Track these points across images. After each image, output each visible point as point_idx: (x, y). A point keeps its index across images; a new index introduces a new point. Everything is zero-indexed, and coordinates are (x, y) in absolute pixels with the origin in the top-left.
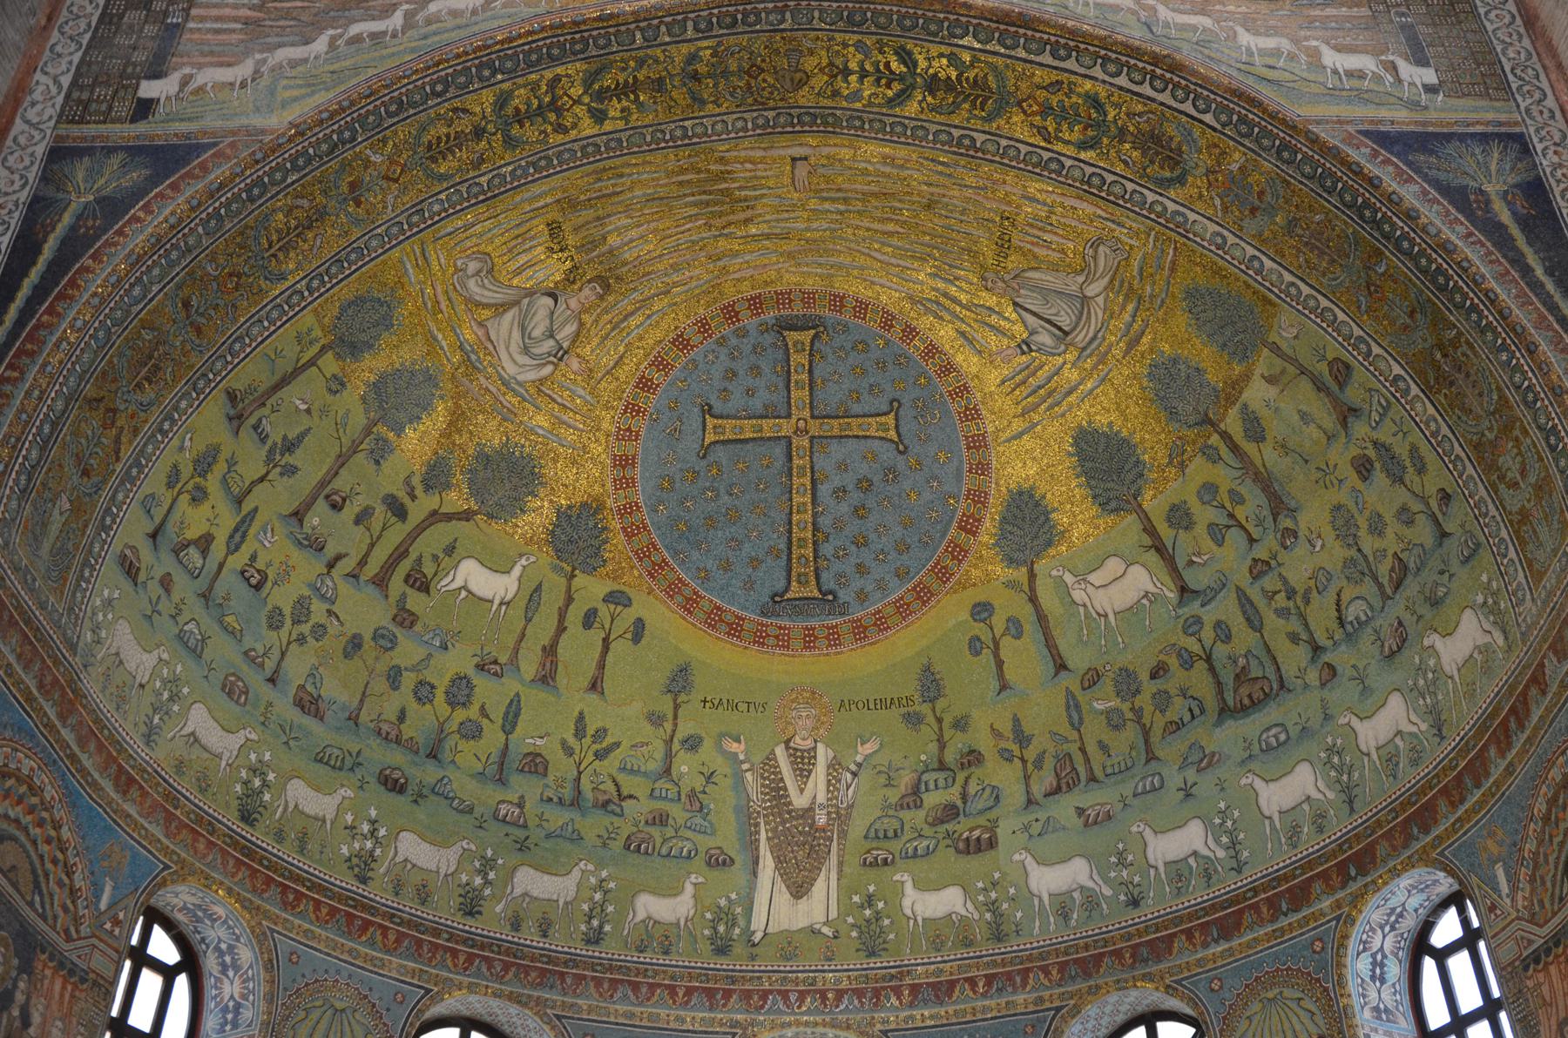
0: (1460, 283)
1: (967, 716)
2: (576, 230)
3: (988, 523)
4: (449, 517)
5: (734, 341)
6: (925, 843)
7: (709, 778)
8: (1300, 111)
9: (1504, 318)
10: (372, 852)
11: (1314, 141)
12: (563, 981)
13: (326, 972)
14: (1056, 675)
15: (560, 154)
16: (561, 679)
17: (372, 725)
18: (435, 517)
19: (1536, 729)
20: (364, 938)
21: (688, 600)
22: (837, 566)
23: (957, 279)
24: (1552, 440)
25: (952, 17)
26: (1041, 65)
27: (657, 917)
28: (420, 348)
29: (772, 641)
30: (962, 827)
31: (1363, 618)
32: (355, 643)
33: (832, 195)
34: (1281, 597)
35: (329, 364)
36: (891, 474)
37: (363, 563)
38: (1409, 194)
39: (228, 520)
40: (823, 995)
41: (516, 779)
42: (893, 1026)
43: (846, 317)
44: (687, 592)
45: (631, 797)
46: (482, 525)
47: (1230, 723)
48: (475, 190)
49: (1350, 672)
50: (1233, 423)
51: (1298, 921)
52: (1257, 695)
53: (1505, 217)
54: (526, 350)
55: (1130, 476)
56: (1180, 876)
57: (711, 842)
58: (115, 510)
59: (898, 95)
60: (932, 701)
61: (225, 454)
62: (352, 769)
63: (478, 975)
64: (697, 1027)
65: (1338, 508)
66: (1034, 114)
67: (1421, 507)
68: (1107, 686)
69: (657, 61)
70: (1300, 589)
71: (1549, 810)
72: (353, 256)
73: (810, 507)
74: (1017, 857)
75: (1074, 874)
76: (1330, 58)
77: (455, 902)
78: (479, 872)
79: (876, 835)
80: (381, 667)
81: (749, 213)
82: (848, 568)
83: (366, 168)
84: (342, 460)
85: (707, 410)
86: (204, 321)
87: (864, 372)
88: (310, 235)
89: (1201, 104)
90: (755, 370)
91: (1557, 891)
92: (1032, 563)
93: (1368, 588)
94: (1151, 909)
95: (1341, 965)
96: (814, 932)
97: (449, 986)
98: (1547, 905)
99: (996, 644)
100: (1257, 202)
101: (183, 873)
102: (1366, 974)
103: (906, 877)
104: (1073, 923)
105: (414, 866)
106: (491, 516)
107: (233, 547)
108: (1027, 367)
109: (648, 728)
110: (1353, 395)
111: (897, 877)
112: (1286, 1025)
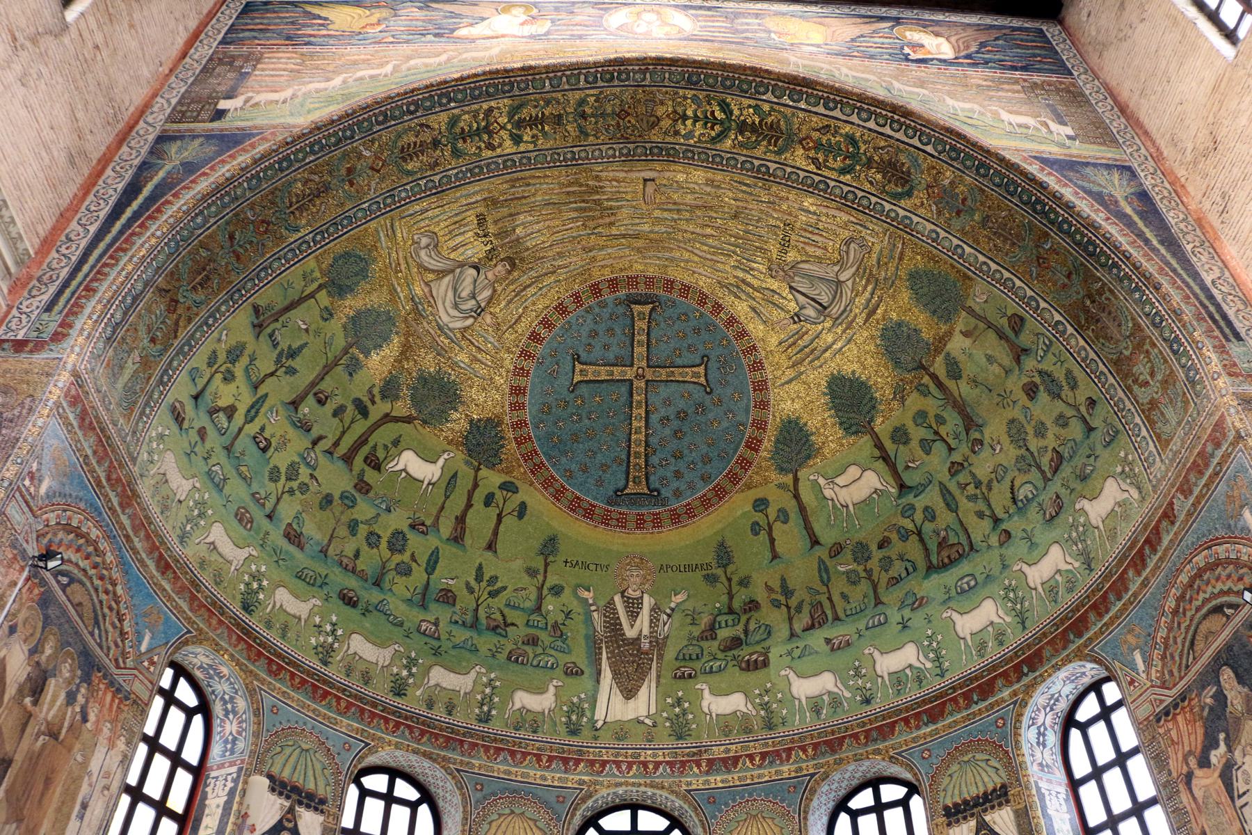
2: (496, 222)
4: (397, 420)
5: (597, 310)
6: (718, 663)
7: (568, 615)
9: (1137, 269)
10: (331, 645)
11: (1002, 160)
12: (462, 746)
15: (488, 165)
16: (468, 541)
18: (387, 418)
19: (1167, 550)
21: (557, 491)
22: (661, 472)
23: (752, 269)
24: (1175, 347)
26: (816, 113)
27: (529, 707)
30: (744, 653)
31: (1030, 496)
32: (327, 500)
33: (670, 206)
34: (971, 489)
36: (700, 407)
38: (1068, 193)
39: (246, 400)
40: (645, 764)
41: (433, 606)
42: (694, 787)
43: (675, 295)
44: (557, 486)
45: (513, 624)
47: (935, 576)
48: (430, 185)
49: (1021, 534)
51: (986, 707)
55: (866, 409)
57: (568, 658)
59: (718, 135)
60: (725, 566)
61: (247, 352)
63: (402, 736)
64: (556, 784)
65: (1012, 421)
66: (809, 149)
67: (1075, 413)
68: (848, 555)
69: (558, 102)
70: (985, 482)
71: (1178, 606)
73: (643, 430)
74: (783, 673)
75: (826, 682)
78: (406, 667)
79: (682, 658)
80: (344, 519)
81: (612, 219)
83: (359, 159)
84: (327, 369)
85: (577, 358)
87: (685, 336)
93: (1034, 475)
94: (877, 706)
95: (1017, 734)
100: (961, 207)
101: (200, 639)
102: (1034, 741)
103: (704, 686)
104: (823, 716)
106: (425, 422)
107: (249, 419)
109: (527, 578)
110: (1025, 339)
111: (698, 686)
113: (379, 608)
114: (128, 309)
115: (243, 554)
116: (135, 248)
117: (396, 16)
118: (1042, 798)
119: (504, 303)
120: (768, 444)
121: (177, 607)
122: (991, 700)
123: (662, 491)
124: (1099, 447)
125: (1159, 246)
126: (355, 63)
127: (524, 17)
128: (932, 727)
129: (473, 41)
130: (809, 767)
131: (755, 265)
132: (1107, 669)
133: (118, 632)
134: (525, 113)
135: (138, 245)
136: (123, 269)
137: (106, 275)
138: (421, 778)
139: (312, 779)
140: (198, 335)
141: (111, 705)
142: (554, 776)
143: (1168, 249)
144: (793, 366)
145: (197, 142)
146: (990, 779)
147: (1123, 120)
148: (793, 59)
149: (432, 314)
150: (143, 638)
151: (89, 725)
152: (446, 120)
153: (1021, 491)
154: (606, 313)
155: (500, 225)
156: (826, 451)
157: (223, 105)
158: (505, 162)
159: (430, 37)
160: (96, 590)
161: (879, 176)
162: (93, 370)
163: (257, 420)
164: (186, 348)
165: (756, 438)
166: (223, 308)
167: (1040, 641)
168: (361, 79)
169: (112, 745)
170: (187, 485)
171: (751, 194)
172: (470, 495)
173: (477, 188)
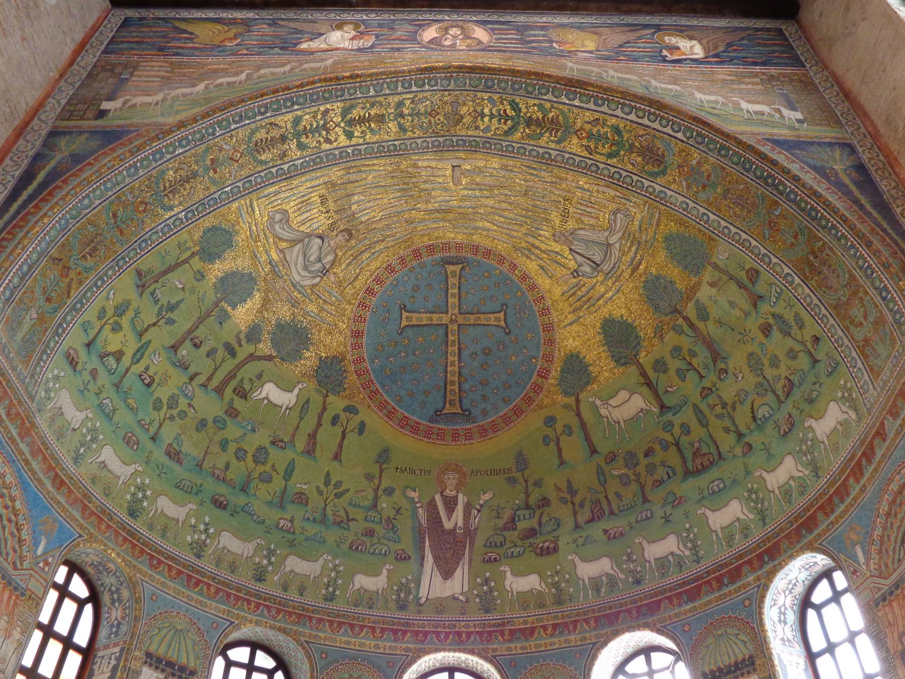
0: (825, 213)
3: (553, 373)
4: (260, 358)
5: (418, 270)
6: (518, 550)
7: (398, 511)
11: (739, 142)
13: (173, 607)
14: (591, 455)
15: (328, 155)
16: (318, 452)
17: (210, 470)
18: (252, 357)
19: (880, 462)
20: (196, 590)
21: (390, 412)
23: (540, 236)
24: (884, 294)
25: (541, 83)
26: (588, 109)
27: (366, 587)
28: (247, 263)
29: (435, 436)
30: (539, 541)
31: (767, 415)
32: (203, 424)
35: (196, 263)
37: (210, 379)
38: (795, 168)
40: (459, 634)
42: (499, 653)
43: (479, 257)
44: (389, 408)
45: (354, 520)
46: (278, 364)
48: (280, 172)
52: (706, 463)
53: (847, 181)
54: (306, 268)
56: (663, 566)
57: (398, 547)
58: (65, 326)
59: (510, 129)
60: (523, 470)
61: (134, 306)
62: (196, 494)
64: (387, 651)
65: (751, 354)
66: (582, 139)
68: (620, 461)
69: (381, 104)
70: (730, 403)
71: (890, 509)
72: (212, 202)
74: (570, 557)
75: (603, 566)
76: (744, 105)
77: (251, 573)
78: (266, 557)
79: (490, 545)
80: (217, 439)
83: (220, 151)
84: (201, 320)
85: (404, 308)
86: (124, 226)
90: (430, 285)
91: (897, 557)
92: (578, 394)
93: (770, 398)
94: (648, 586)
95: (761, 614)
96: (454, 598)
98: (891, 566)
99: (558, 439)
100: (706, 182)
102: (776, 619)
104: (602, 594)
105: (228, 551)
107: (136, 360)
108: (577, 285)
110: (760, 288)
111: (502, 569)
112: (730, 650)
114: (24, 275)
115: (131, 469)
116: (30, 225)
117: (249, 31)
118: (784, 668)
119: (343, 267)
120: (555, 373)
123: (473, 411)
125: (871, 210)
126: (215, 71)
127: (353, 33)
128: (690, 606)
129: (312, 53)
131: (542, 232)
132: (834, 560)
134: (355, 113)
135: (32, 223)
136: (19, 243)
138: (277, 649)
139: (185, 655)
140: (89, 294)
141: (8, 601)
142: (386, 644)
143: (880, 213)
145: (83, 137)
146: (740, 650)
147: (846, 104)
148: (570, 64)
150: (39, 544)
152: (291, 120)
153: (760, 411)
155: (339, 202)
157: (105, 105)
158: (340, 153)
163: (142, 361)
164: (78, 306)
165: (545, 369)
168: (221, 85)
170: (80, 416)
171: (537, 176)
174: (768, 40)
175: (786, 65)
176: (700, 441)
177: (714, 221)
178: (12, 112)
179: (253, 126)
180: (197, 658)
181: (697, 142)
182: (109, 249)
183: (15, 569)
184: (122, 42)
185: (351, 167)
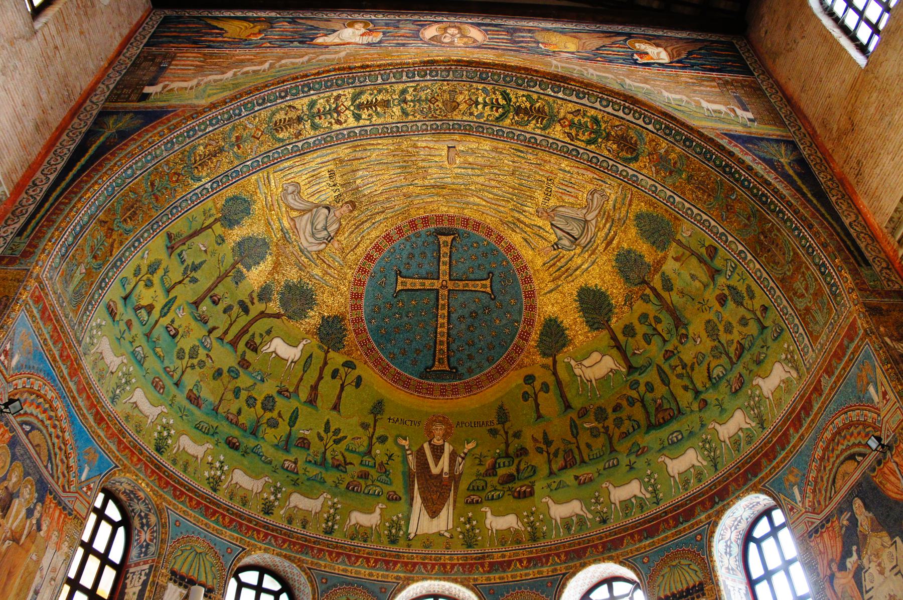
1: (521, 431)
5: (414, 239)
7: (390, 457)
8: (694, 123)
10: (220, 477)
11: (701, 135)
15: (337, 135)
18: (262, 315)
19: (816, 414)
21: (384, 368)
22: (458, 355)
23: (525, 211)
24: (823, 270)
27: (361, 523)
30: (517, 486)
32: (219, 373)
35: (218, 228)
37: (226, 333)
39: (161, 301)
40: (444, 565)
41: (293, 450)
42: (479, 582)
43: (469, 229)
45: (351, 464)
46: (285, 322)
48: (295, 149)
50: (657, 282)
53: (791, 172)
54: (313, 235)
55: (605, 312)
59: (501, 116)
61: (162, 266)
62: (213, 435)
63: (270, 543)
64: (380, 579)
65: (709, 322)
66: (565, 126)
69: (387, 91)
70: (689, 364)
71: (824, 454)
73: (446, 325)
74: (544, 500)
75: (574, 508)
77: (260, 507)
78: (273, 493)
79: (472, 489)
80: (231, 386)
82: (464, 357)
83: (244, 130)
84: (220, 279)
85: (399, 273)
87: (477, 258)
88: (215, 160)
89: (647, 120)
90: (423, 254)
93: (724, 360)
94: (612, 525)
95: (710, 546)
96: (441, 535)
97: (255, 548)
99: (536, 395)
103: (488, 509)
104: (572, 532)
106: (289, 317)
107: (163, 314)
109: (361, 429)
110: (718, 263)
111: (483, 509)
113: (255, 451)
114: (77, 235)
115: (158, 410)
117: (272, 27)
119: (346, 235)
120: (535, 336)
121: (108, 448)
122: (693, 521)
123: (460, 369)
124: (769, 340)
125: (812, 198)
126: (242, 61)
127: (363, 30)
128: (650, 541)
129: (327, 47)
130: (561, 568)
131: (527, 209)
132: (774, 499)
133: (65, 466)
134: (364, 98)
136: (74, 207)
137: (62, 210)
139: (204, 575)
140: (127, 254)
141: (59, 519)
142: (379, 574)
143: (818, 200)
144: (553, 281)
145: (128, 117)
146: (691, 578)
147: (789, 108)
148: (554, 62)
149: (296, 241)
151: (42, 533)
152: (307, 103)
154: (420, 242)
155: (345, 177)
156: (576, 342)
157: (147, 90)
159: (296, 44)
160: (50, 435)
161: (615, 146)
162: (51, 278)
166: (146, 235)
167: (728, 479)
168: (247, 73)
169: (58, 548)
170: (117, 361)
171: (523, 158)
172: (322, 370)
173: (329, 151)
174: (722, 50)
175: (739, 73)
176: (662, 397)
177: (679, 202)
178: (69, 96)
179: (274, 108)
180: (215, 578)
181: (666, 134)
182: (147, 214)
183: (64, 491)
184: (162, 37)
185: (358, 146)
